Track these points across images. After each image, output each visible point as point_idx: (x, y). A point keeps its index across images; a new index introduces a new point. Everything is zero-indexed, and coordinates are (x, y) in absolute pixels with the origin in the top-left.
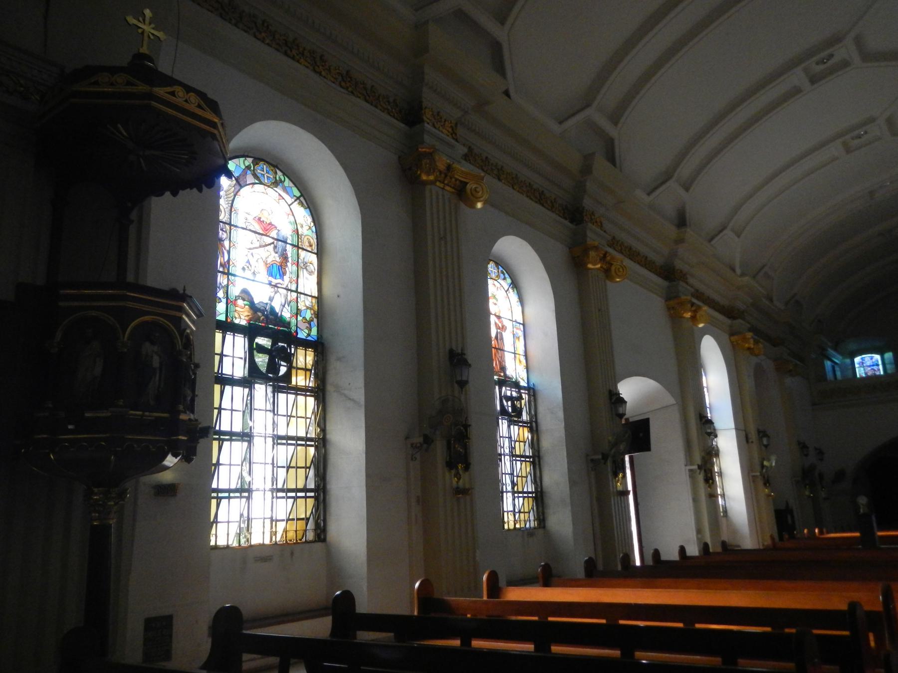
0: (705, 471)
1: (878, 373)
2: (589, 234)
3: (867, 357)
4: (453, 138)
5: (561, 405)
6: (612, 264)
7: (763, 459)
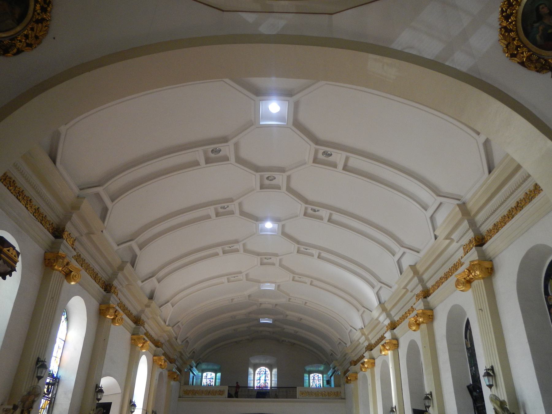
2: (112, 299)
3: (209, 373)
4: (72, 247)
5: (72, 390)
6: (117, 316)
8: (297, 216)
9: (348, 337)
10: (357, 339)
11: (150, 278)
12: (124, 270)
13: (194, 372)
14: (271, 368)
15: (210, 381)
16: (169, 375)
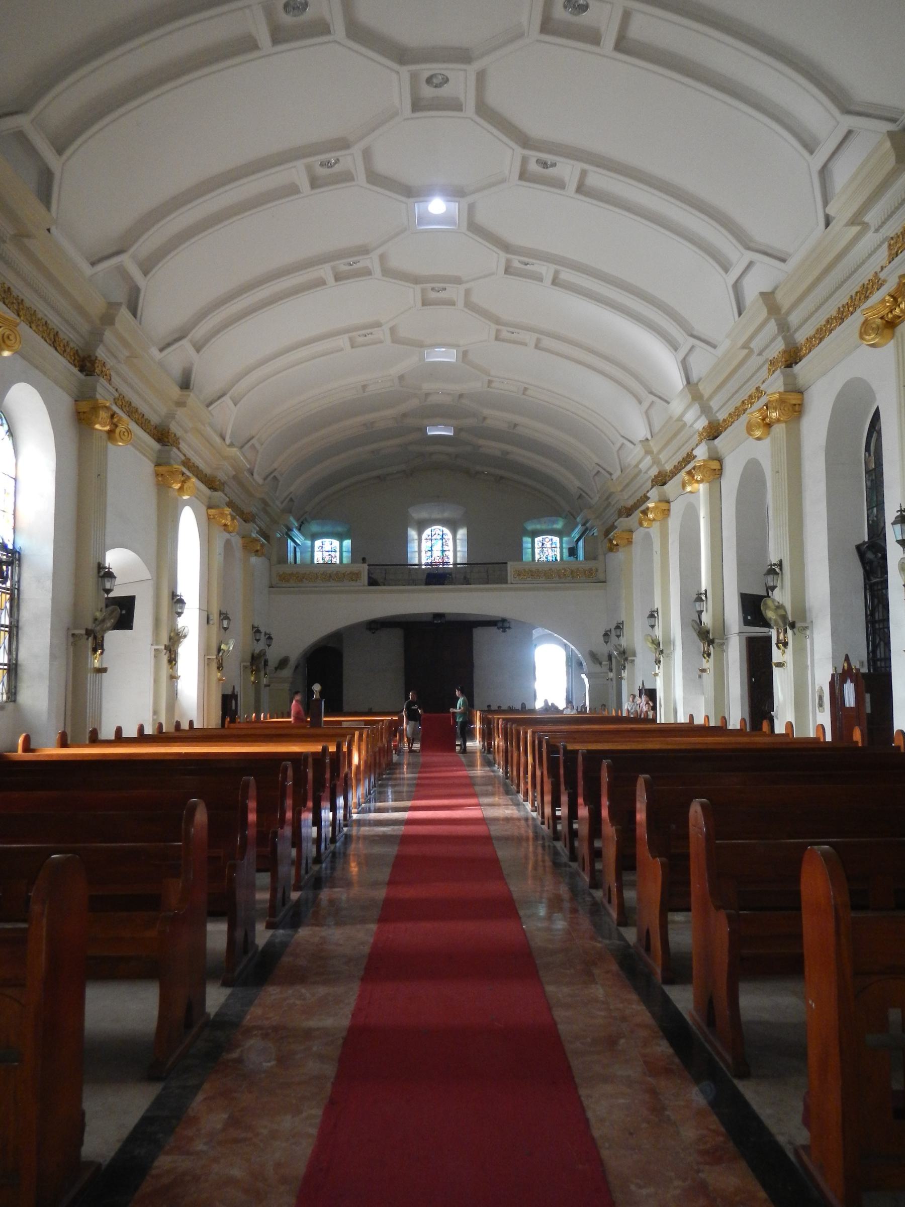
0: (170, 652)
1: (334, 561)
2: (99, 389)
6: (116, 426)
7: (221, 643)
8: (503, 181)
9: (617, 460)
10: (634, 463)
12: (116, 324)
13: (296, 540)
14: (453, 526)
15: (330, 555)
16: (245, 545)
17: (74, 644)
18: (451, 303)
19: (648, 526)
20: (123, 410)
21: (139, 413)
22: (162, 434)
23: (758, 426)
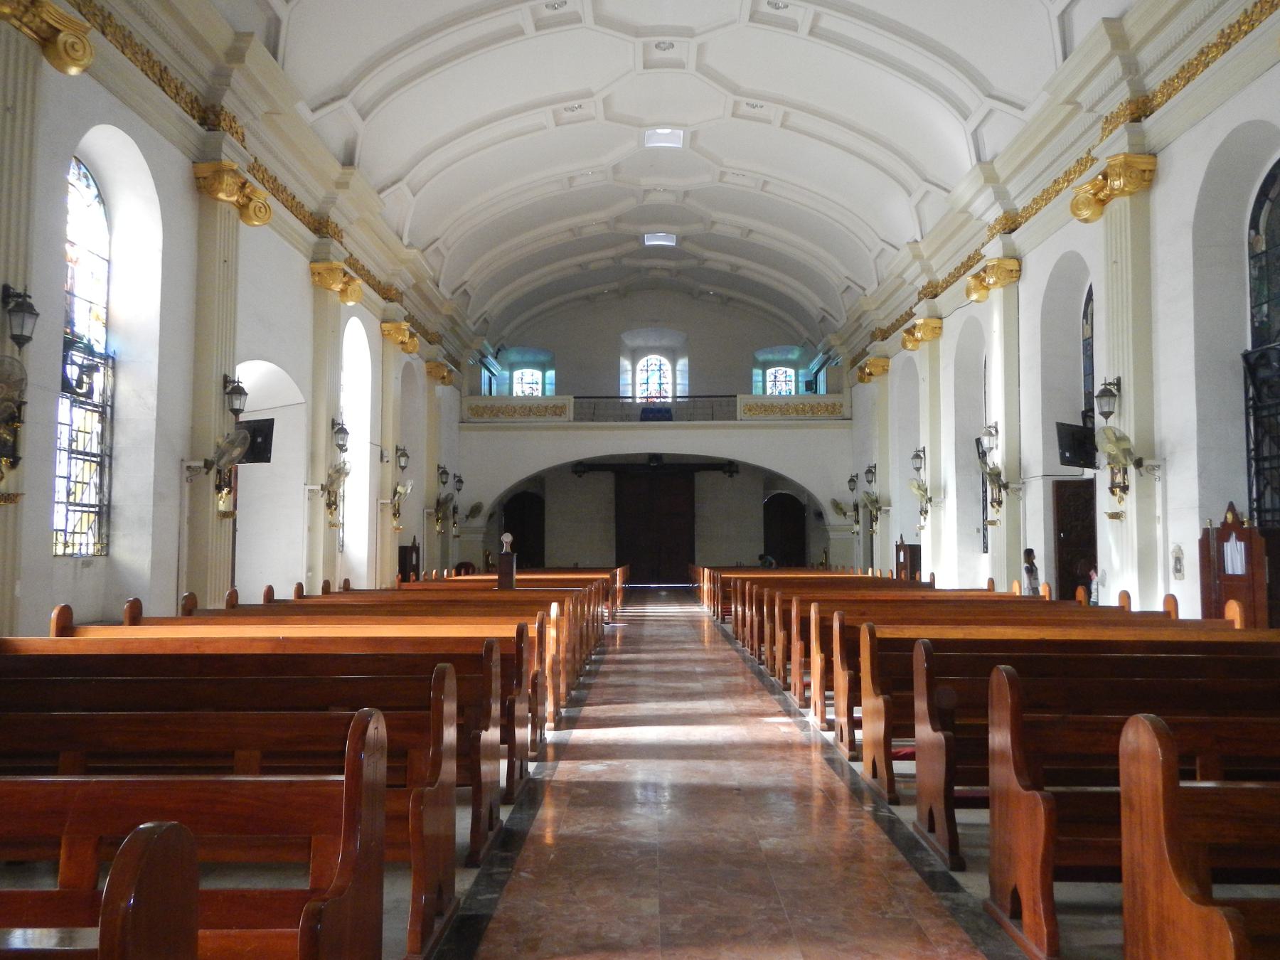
1: (535, 394)
2: (225, 148)
5: (155, 388)
6: (250, 200)
7: (398, 485)
11: (333, 100)
12: (246, 62)
14: (673, 355)
16: (430, 370)
17: (190, 480)
18: (680, 65)
19: (914, 348)
20: (265, 186)
21: (289, 193)
22: (320, 224)
23: (1087, 204)
